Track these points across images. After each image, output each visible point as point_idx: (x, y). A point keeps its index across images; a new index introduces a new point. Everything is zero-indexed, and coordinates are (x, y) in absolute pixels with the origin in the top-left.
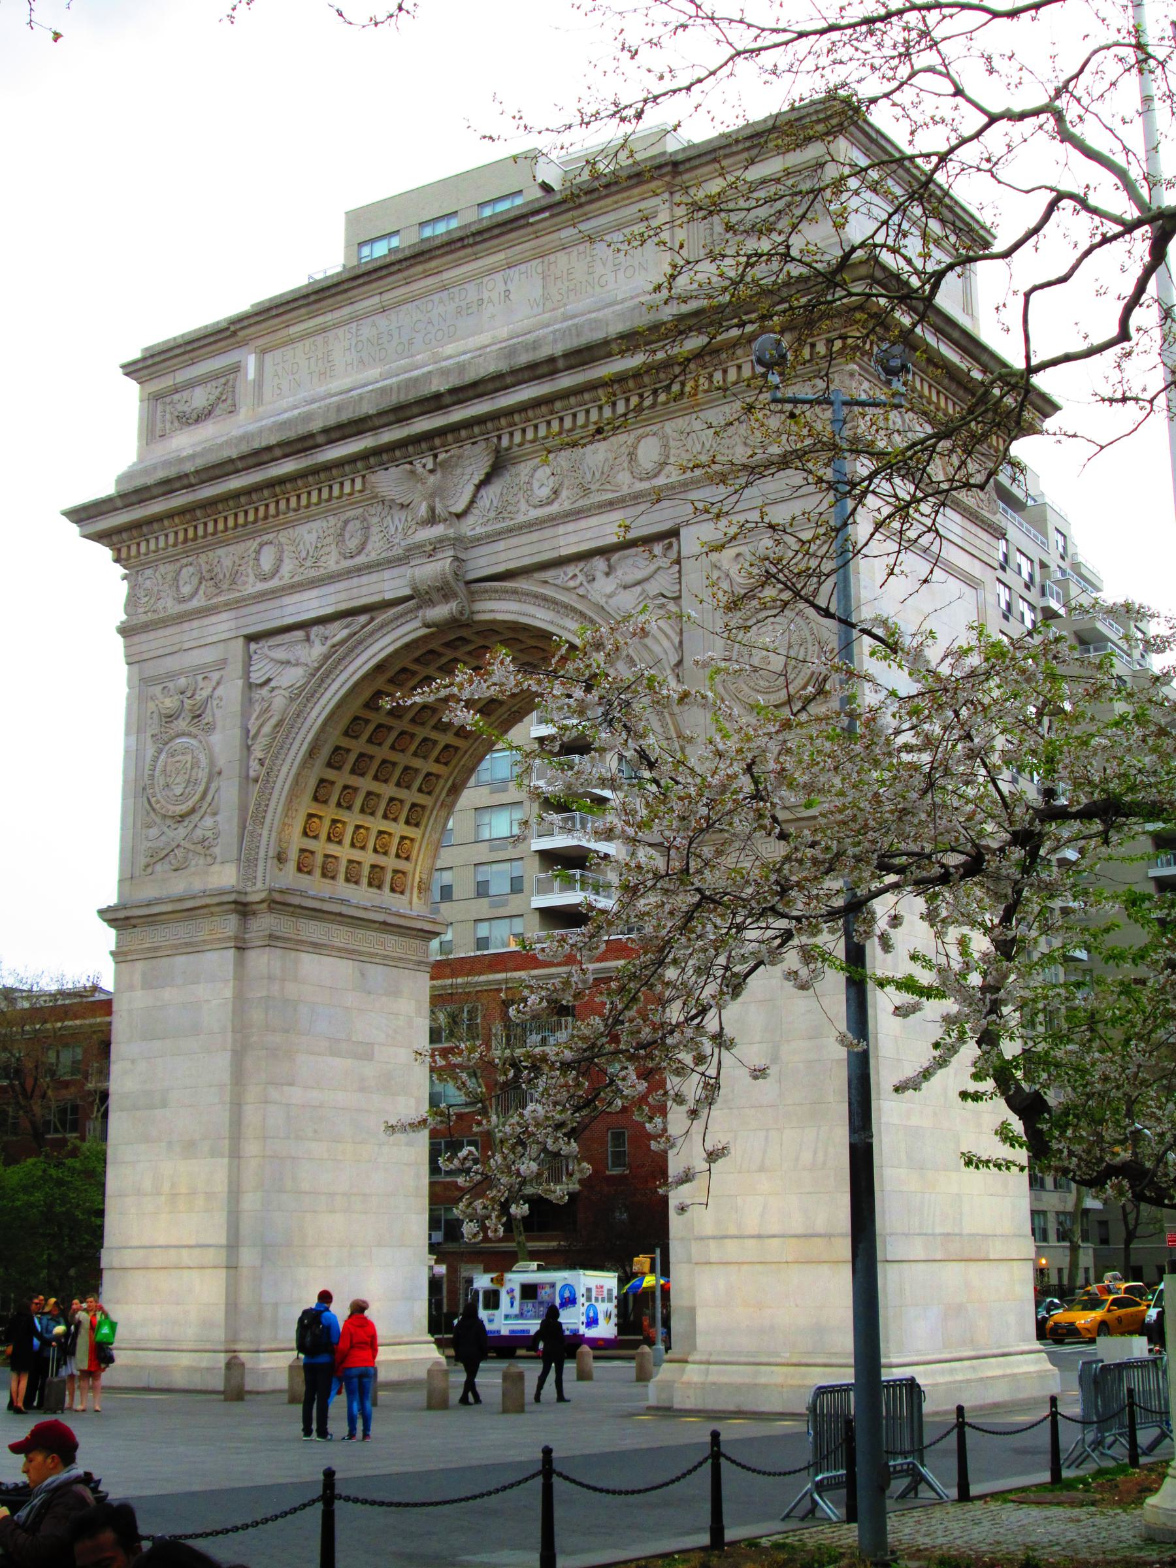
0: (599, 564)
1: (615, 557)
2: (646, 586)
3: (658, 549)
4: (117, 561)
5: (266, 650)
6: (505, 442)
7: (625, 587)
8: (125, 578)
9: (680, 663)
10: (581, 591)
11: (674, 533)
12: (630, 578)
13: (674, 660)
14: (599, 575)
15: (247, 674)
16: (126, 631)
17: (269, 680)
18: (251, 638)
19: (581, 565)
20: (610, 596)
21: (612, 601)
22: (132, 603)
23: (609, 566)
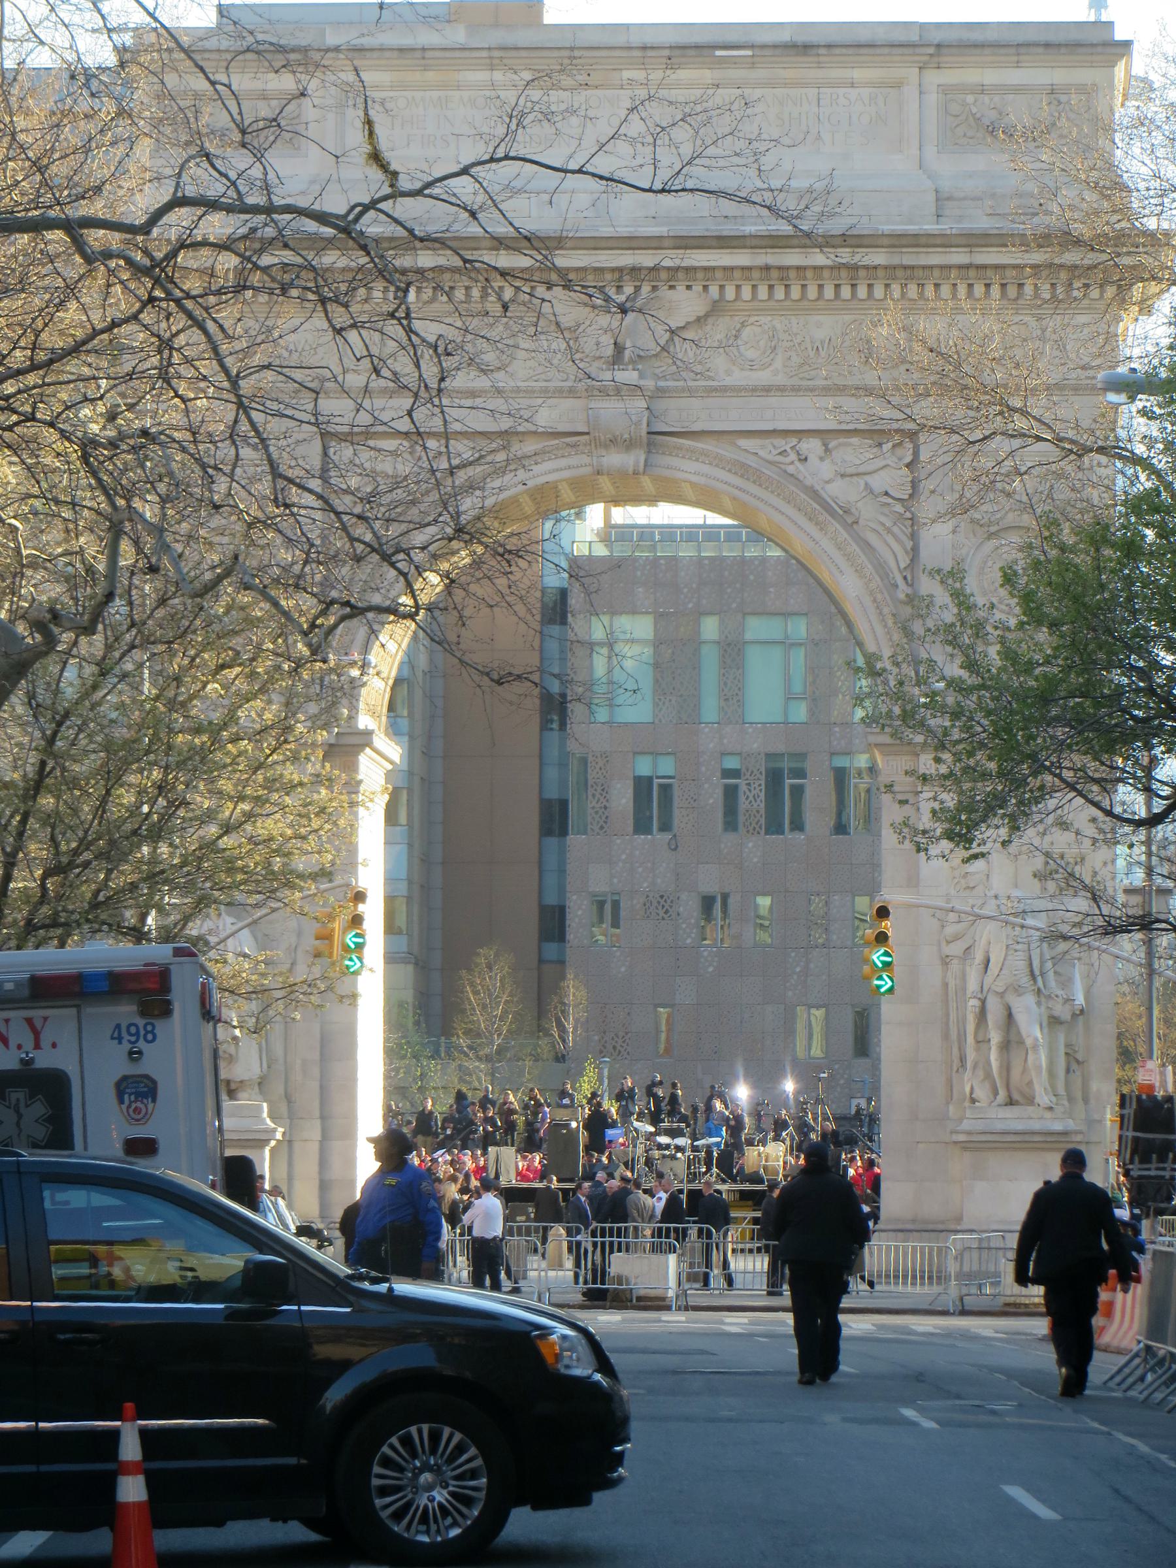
7: (843, 476)
10: (791, 469)
14: (813, 460)
19: (794, 441)
20: (828, 482)
21: (829, 487)
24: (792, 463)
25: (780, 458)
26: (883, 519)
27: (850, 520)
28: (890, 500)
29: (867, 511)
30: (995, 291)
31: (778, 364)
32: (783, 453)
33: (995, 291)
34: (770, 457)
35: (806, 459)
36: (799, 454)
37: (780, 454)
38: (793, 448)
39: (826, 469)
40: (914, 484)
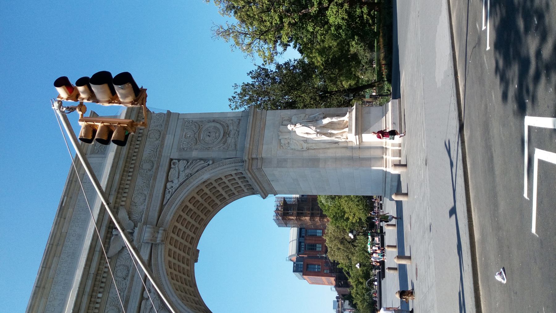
0: (169, 185)
1: (169, 180)
3: (172, 166)
7: (178, 177)
10: (174, 190)
11: (171, 160)
12: (177, 176)
13: (202, 162)
20: (179, 181)
23: (171, 181)
24: (172, 190)
25: (170, 193)
27: (190, 176)
28: (187, 166)
29: (188, 171)
31: (146, 193)
32: (169, 192)
34: (170, 195)
36: (170, 188)
37: (169, 193)
38: (168, 190)
39: (176, 181)
40: (184, 160)
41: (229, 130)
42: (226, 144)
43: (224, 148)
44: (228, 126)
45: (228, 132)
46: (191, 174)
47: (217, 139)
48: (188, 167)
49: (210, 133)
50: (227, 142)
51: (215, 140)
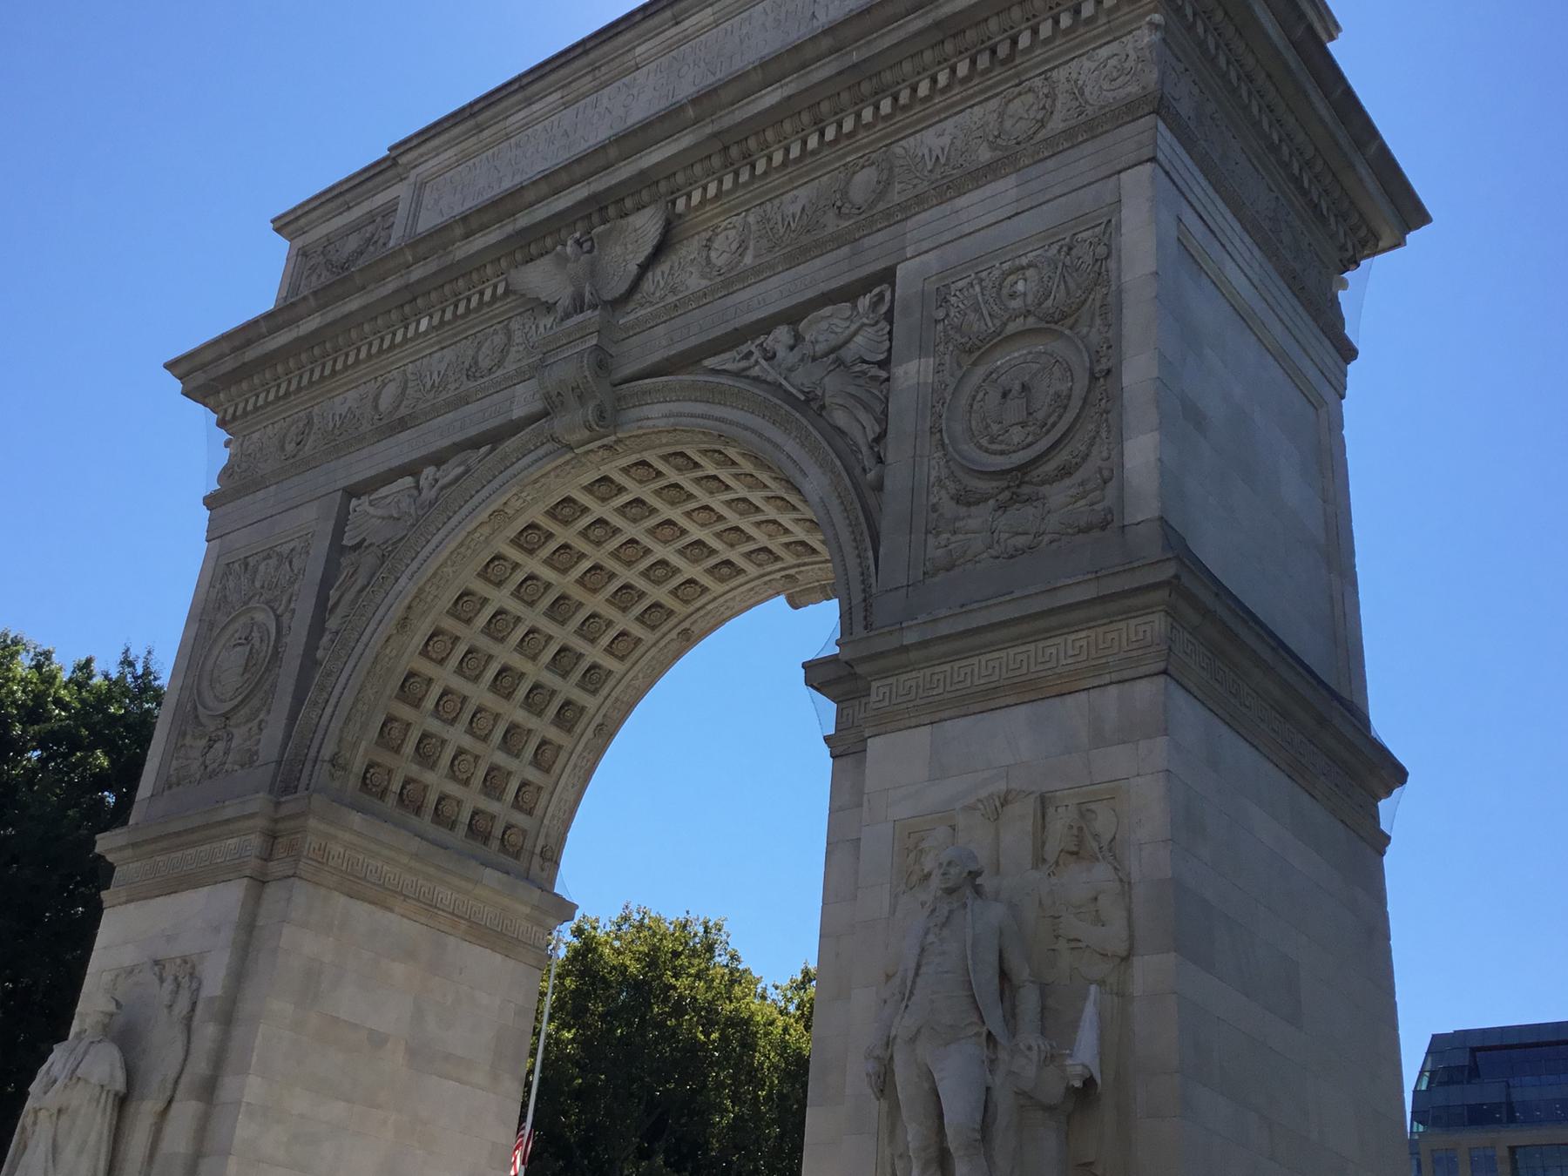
0: (782, 334)
2: (842, 352)
3: (864, 302)
4: (222, 423)
5: (366, 506)
6: (681, 204)
8: (227, 444)
9: (880, 438)
10: (756, 371)
15: (339, 532)
16: (211, 502)
17: (364, 540)
18: (352, 492)
20: (791, 370)
22: (227, 473)
24: (757, 362)
25: (744, 364)
26: (852, 389)
27: (815, 405)
30: (983, 61)
33: (983, 61)
35: (775, 355)
41: (1045, 489)
42: (963, 511)
43: (934, 508)
44: (1065, 472)
45: (1026, 490)
46: (823, 407)
47: (986, 451)
48: (864, 373)
49: (1024, 387)
50: (973, 509)
51: (984, 442)
